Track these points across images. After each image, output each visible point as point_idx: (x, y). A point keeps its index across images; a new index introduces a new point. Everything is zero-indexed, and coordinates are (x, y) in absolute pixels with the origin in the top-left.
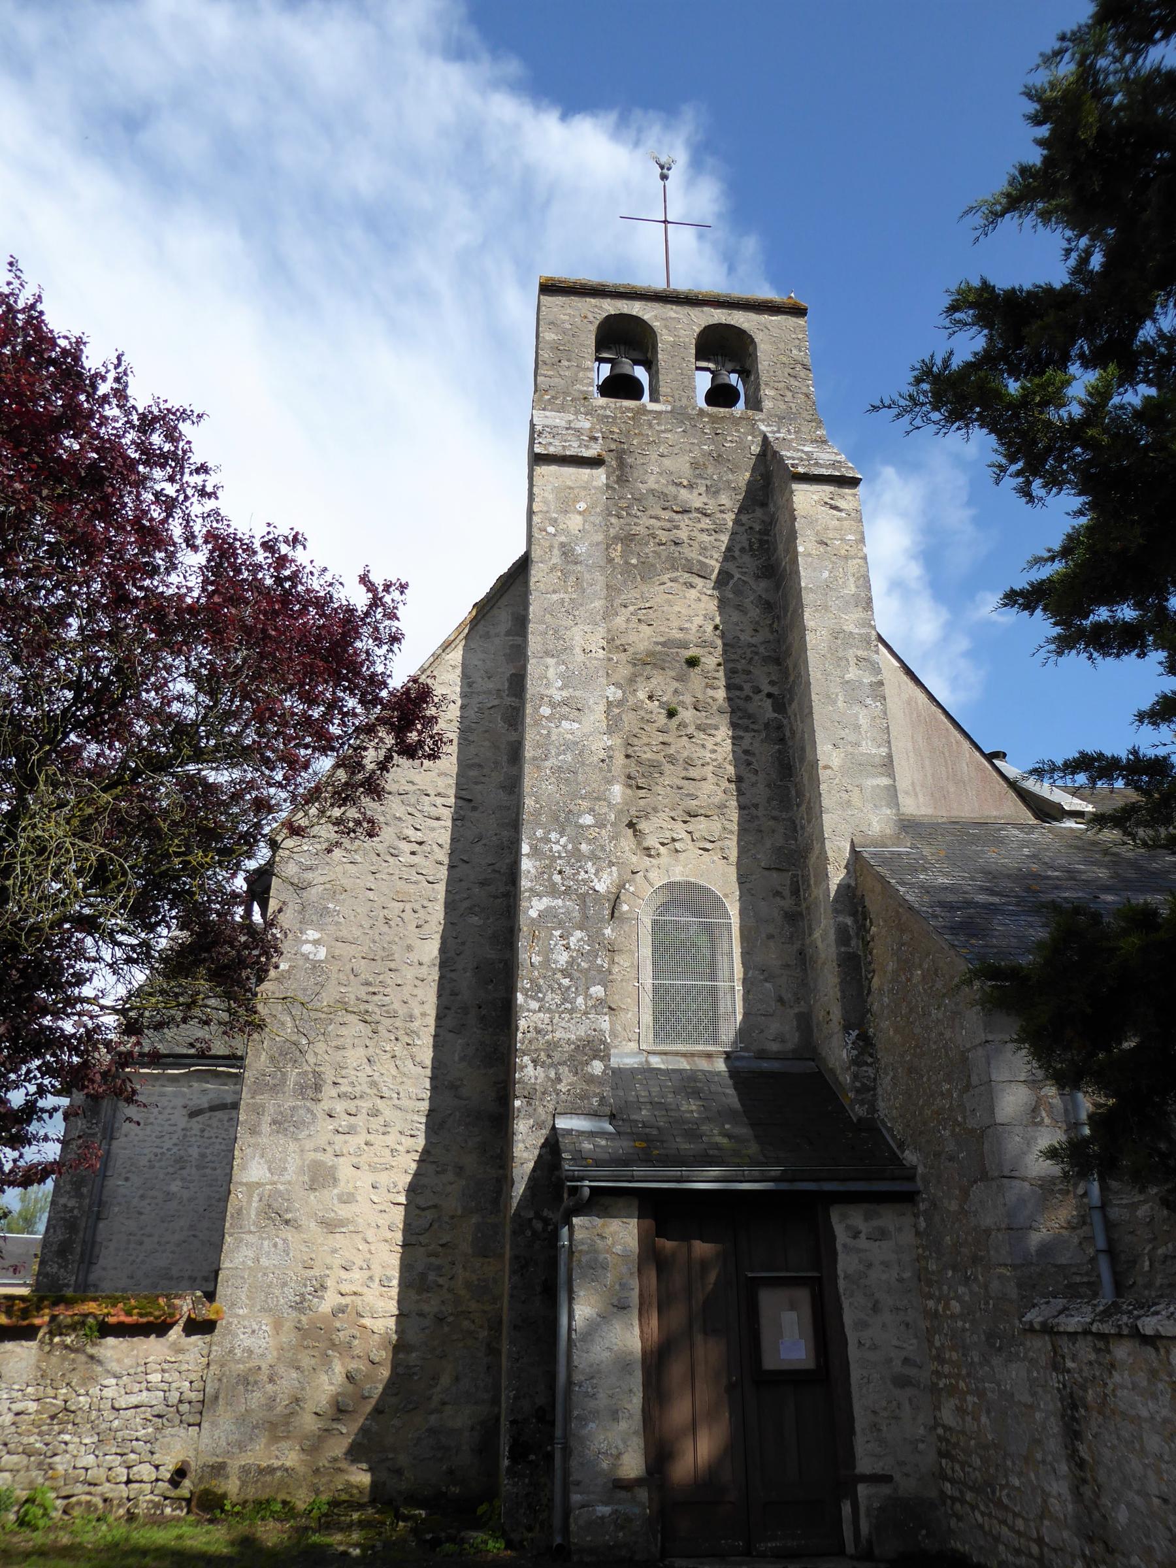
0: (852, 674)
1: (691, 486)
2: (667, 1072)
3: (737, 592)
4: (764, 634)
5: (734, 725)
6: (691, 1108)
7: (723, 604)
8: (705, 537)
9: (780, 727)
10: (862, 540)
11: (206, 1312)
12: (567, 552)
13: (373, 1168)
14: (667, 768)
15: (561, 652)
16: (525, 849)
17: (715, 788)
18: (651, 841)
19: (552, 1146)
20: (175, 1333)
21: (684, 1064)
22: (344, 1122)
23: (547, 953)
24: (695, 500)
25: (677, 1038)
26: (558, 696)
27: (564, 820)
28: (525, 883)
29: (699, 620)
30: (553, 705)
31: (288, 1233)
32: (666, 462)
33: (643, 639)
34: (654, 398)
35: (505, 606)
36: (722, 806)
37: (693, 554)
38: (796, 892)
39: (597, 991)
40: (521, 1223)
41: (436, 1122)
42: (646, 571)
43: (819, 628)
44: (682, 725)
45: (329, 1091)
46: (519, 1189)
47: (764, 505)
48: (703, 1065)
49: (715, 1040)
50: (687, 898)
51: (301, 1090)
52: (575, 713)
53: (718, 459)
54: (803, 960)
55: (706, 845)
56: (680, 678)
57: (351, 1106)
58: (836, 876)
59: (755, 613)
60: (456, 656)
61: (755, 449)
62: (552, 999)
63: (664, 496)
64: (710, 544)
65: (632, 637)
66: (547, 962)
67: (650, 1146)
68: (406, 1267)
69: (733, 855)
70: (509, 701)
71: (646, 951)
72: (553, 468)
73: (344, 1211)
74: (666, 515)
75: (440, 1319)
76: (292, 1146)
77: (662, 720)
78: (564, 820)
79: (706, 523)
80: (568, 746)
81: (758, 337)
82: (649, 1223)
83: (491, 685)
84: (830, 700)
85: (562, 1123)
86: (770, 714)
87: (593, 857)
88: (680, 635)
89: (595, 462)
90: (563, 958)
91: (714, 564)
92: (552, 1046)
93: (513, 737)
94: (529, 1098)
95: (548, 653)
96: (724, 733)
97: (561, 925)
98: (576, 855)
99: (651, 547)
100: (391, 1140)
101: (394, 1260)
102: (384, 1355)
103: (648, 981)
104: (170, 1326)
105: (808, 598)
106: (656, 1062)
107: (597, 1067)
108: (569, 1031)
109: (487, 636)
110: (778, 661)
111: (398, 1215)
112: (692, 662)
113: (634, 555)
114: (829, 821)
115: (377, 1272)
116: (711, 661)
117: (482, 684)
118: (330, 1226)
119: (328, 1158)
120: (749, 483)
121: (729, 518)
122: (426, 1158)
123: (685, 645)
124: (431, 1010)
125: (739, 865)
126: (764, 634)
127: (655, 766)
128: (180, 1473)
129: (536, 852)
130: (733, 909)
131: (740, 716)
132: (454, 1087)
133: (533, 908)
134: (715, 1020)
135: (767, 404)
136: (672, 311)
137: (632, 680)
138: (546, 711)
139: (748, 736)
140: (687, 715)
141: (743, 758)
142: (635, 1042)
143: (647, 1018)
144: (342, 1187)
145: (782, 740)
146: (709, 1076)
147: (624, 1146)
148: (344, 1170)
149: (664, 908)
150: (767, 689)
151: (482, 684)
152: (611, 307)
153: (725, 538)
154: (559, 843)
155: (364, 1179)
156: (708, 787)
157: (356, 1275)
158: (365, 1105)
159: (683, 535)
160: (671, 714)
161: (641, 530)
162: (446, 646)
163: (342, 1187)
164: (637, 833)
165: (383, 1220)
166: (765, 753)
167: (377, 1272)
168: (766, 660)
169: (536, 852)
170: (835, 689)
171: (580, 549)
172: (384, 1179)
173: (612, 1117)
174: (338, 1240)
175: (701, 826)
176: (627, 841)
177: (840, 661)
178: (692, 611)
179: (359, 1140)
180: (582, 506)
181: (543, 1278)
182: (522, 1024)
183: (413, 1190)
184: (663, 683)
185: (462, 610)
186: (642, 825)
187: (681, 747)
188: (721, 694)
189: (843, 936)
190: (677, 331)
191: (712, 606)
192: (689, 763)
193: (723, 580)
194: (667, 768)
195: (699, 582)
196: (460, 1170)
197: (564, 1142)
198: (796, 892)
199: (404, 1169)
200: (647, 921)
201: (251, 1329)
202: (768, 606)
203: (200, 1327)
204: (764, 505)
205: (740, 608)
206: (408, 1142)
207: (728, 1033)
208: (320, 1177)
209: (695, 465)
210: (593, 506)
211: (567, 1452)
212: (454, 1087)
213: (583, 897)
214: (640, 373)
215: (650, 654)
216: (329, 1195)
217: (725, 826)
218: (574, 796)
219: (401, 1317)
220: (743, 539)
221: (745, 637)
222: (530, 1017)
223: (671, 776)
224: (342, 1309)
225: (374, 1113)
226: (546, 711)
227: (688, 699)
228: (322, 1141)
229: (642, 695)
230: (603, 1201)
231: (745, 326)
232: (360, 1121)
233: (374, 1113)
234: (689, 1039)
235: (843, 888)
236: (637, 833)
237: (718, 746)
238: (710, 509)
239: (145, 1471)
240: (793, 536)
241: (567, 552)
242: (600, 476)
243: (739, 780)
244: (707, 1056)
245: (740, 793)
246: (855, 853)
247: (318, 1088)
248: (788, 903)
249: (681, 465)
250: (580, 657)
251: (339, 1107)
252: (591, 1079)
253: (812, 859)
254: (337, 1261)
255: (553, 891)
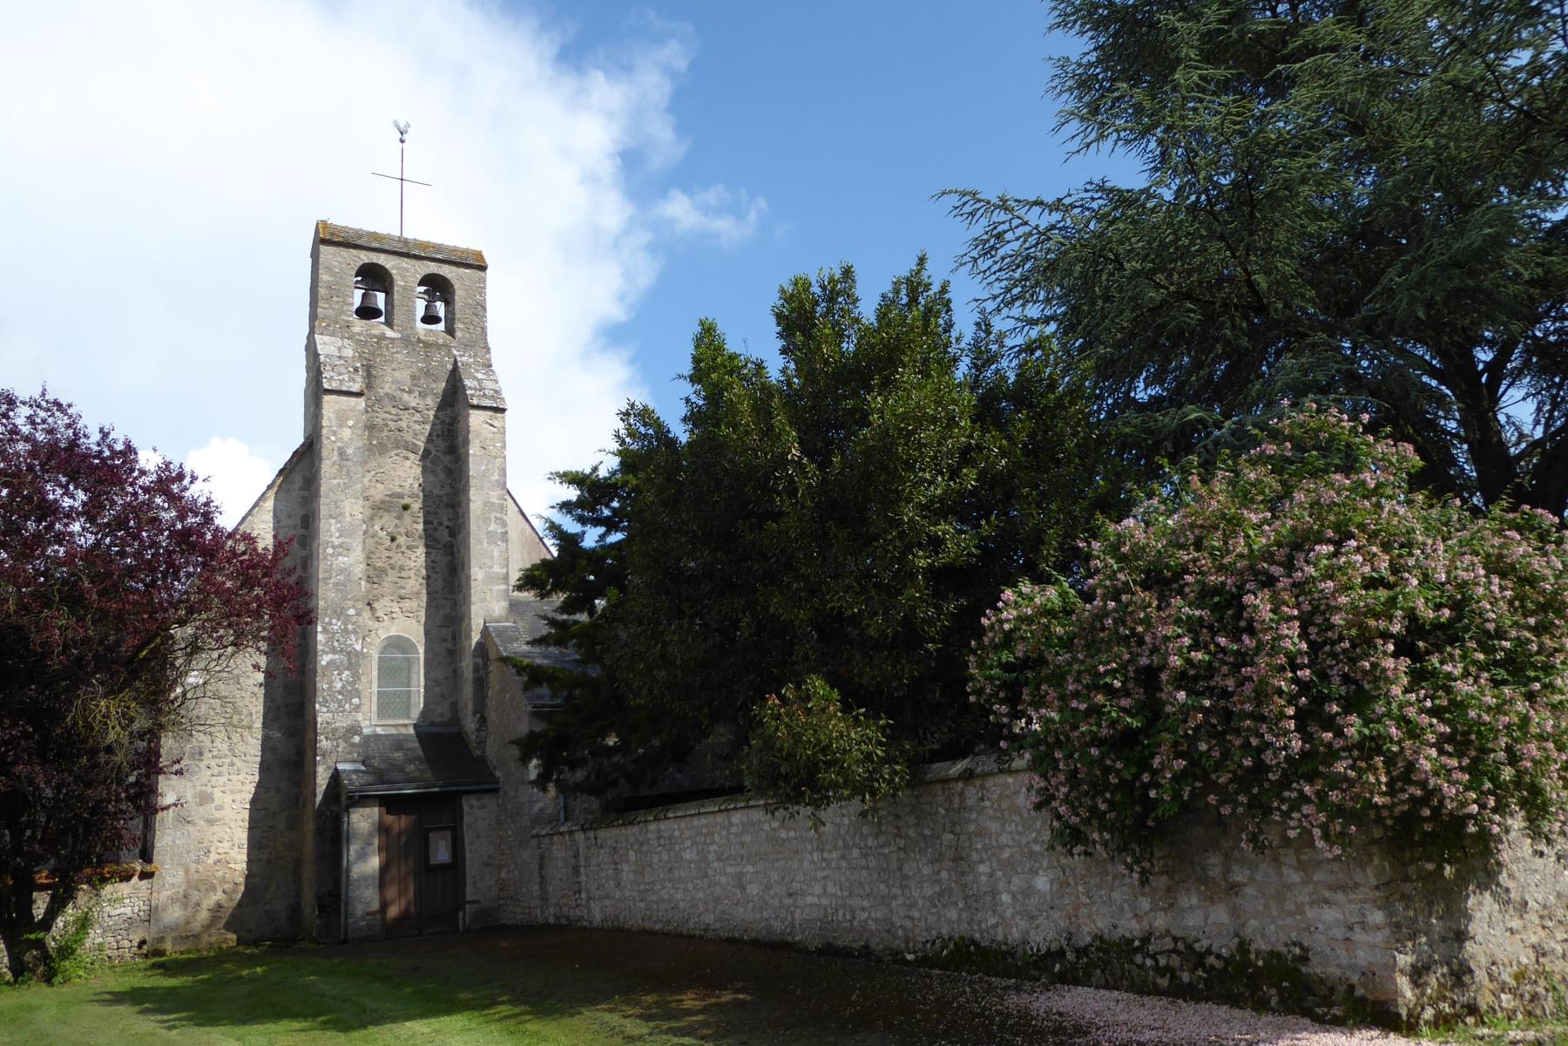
0: (493, 527)
1: (410, 392)
2: (386, 736)
3: (434, 463)
4: (447, 489)
5: (427, 546)
6: (399, 755)
7: (425, 470)
8: (417, 427)
9: (452, 546)
10: (504, 447)
11: (148, 868)
12: (342, 453)
13: (232, 792)
14: (390, 572)
15: (338, 516)
16: (319, 629)
17: (415, 583)
18: (380, 614)
19: (336, 777)
20: (135, 879)
21: (393, 731)
22: (216, 770)
23: (331, 683)
24: (412, 401)
25: (390, 717)
26: (337, 542)
27: (339, 613)
28: (320, 647)
29: (410, 481)
30: (334, 547)
31: (190, 828)
32: (396, 373)
33: (379, 492)
34: (389, 323)
35: (301, 474)
36: (418, 593)
37: (408, 437)
38: (454, 638)
39: (355, 701)
40: (319, 813)
41: (264, 768)
42: (382, 449)
43: (478, 500)
44: (399, 546)
45: (207, 755)
46: (319, 798)
47: (452, 406)
48: (403, 731)
49: (408, 717)
50: (398, 644)
51: (192, 756)
52: (343, 551)
53: (427, 374)
54: (456, 675)
55: (408, 614)
56: (399, 518)
57: (220, 762)
58: (476, 638)
59: (442, 476)
60: (269, 504)
61: (449, 367)
62: (334, 706)
63: (393, 398)
64: (418, 430)
65: (372, 492)
66: (330, 688)
67: (381, 777)
68: (250, 838)
69: (423, 620)
70: (301, 531)
71: (375, 673)
72: (334, 397)
73: (217, 815)
74: (394, 411)
75: (269, 862)
76: (189, 784)
77: (388, 543)
78: (339, 613)
79: (418, 417)
80: (342, 571)
81: (457, 285)
82: (384, 810)
83: (290, 522)
84: (480, 542)
85: (340, 767)
86: (447, 538)
87: (354, 632)
88: (398, 490)
89: (359, 395)
90: (339, 685)
91: (421, 444)
92: (335, 730)
93: (304, 553)
94: (323, 756)
95: (331, 516)
96: (421, 550)
97: (337, 668)
98: (346, 631)
99: (385, 434)
100: (241, 777)
101: (245, 835)
102: (241, 880)
103: (375, 689)
104: (132, 876)
105: (473, 482)
106: (379, 730)
107: (357, 739)
108: (342, 723)
109: (288, 491)
110: (453, 507)
111: (246, 814)
112: (406, 508)
113: (378, 441)
114: (474, 608)
115: (236, 842)
116: (416, 506)
117: (285, 521)
118: (211, 822)
119: (209, 789)
120: (445, 391)
121: (432, 413)
122: (259, 786)
123: (401, 496)
124: (261, 708)
125: (426, 625)
126: (447, 489)
127: (383, 571)
128: (142, 943)
129: (325, 630)
130: (421, 650)
131: (431, 540)
132: (273, 749)
133: (324, 660)
134: (408, 707)
135: (459, 334)
136: (405, 263)
137: (372, 518)
138: (330, 551)
139: (434, 552)
140: (401, 540)
141: (431, 565)
142: (370, 721)
143: (375, 708)
144: (217, 802)
145: (452, 554)
146: (406, 737)
147: (370, 778)
148: (217, 794)
149: (385, 649)
150: (446, 523)
151: (285, 521)
152: (366, 257)
153: (428, 427)
154: (337, 625)
155: (228, 798)
156: (412, 582)
157: (226, 844)
158: (227, 761)
159: (403, 424)
160: (393, 539)
161: (379, 421)
162: (263, 497)
163: (217, 802)
164: (372, 609)
165: (239, 818)
166: (443, 560)
167: (236, 842)
168: (447, 506)
169: (325, 630)
170: (483, 536)
171: (350, 451)
172: (238, 797)
173: (363, 763)
174: (216, 828)
175: (407, 604)
176: (367, 614)
177: (487, 520)
178: (407, 474)
179: (222, 779)
180: (351, 423)
181: (333, 837)
182: (319, 719)
183: (253, 802)
184: (388, 520)
185: (270, 476)
186: (376, 605)
187: (397, 559)
188: (420, 527)
189: (476, 668)
190: (408, 275)
191: (418, 470)
192: (402, 568)
193: (426, 455)
194: (390, 572)
195: (412, 456)
196: (278, 790)
197: (343, 776)
198: (454, 638)
199: (249, 791)
200: (376, 656)
201: (171, 874)
202: (450, 472)
203: (146, 875)
204: (452, 406)
205: (434, 473)
206: (250, 778)
207: (415, 713)
208: (205, 799)
209: (413, 377)
210: (357, 423)
211: (347, 904)
212: (273, 749)
213: (349, 654)
214: (380, 298)
215: (383, 502)
216: (210, 807)
217: (419, 604)
218: (345, 599)
219: (249, 862)
220: (438, 427)
221: (436, 491)
222: (323, 715)
223: (392, 576)
224: (219, 861)
225: (232, 764)
226: (330, 551)
227: (403, 530)
228: (204, 781)
229: (377, 528)
230: (362, 800)
231: (449, 276)
232: (224, 769)
233: (232, 764)
234: (395, 717)
235: (478, 644)
236: (372, 609)
237: (418, 558)
238: (421, 407)
239: (126, 943)
240: (467, 442)
241: (342, 453)
242: (361, 403)
243: (428, 578)
244: (404, 725)
245: (428, 585)
246: (486, 628)
247: (201, 754)
248: (449, 645)
249: (404, 376)
250: (349, 519)
251: (213, 763)
252: (353, 745)
253: (464, 625)
254: (215, 839)
255: (334, 651)
